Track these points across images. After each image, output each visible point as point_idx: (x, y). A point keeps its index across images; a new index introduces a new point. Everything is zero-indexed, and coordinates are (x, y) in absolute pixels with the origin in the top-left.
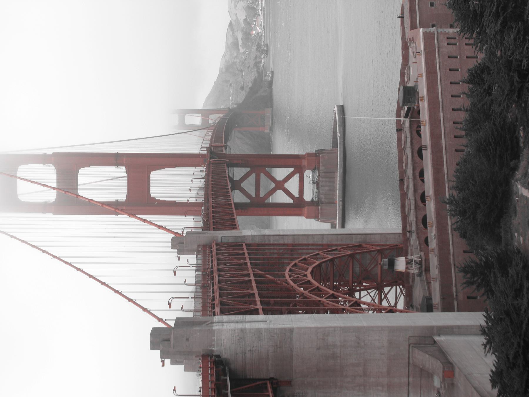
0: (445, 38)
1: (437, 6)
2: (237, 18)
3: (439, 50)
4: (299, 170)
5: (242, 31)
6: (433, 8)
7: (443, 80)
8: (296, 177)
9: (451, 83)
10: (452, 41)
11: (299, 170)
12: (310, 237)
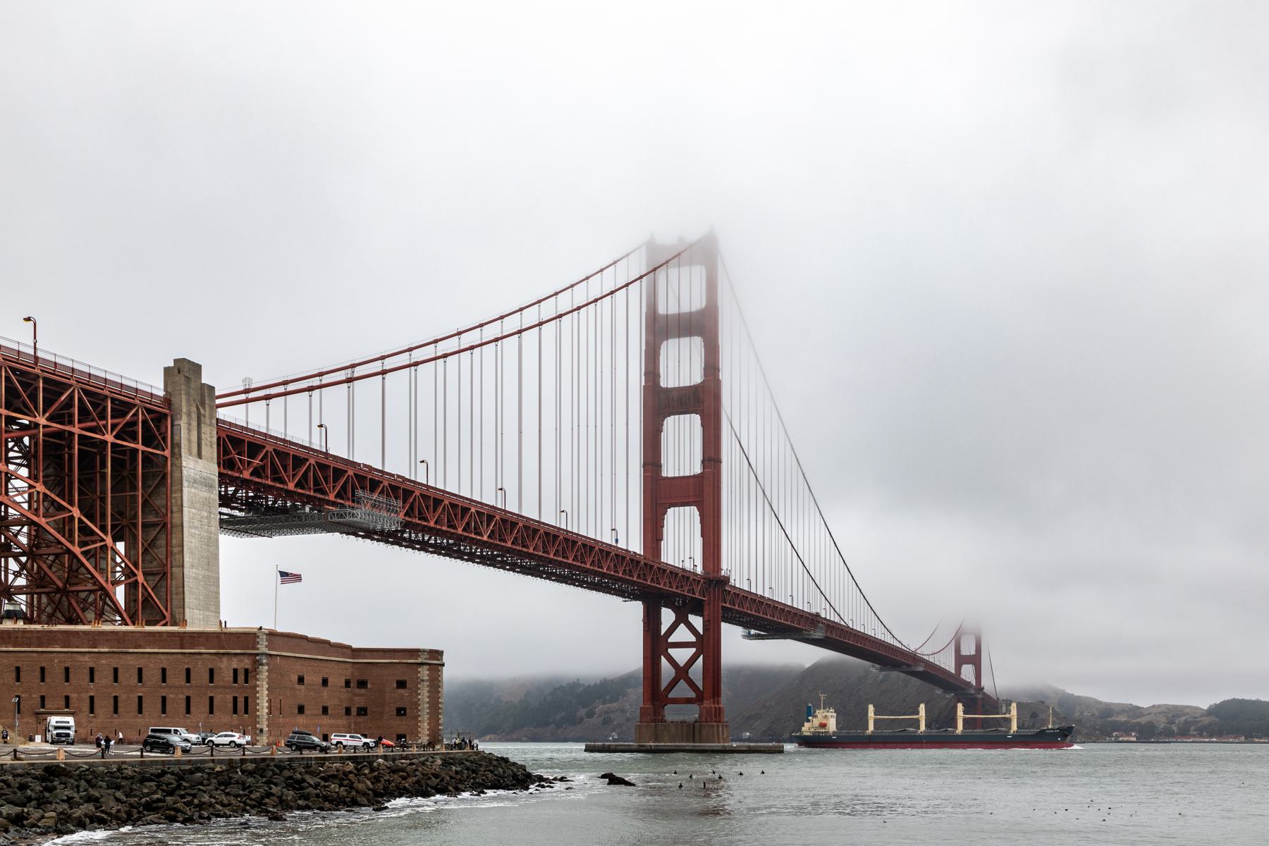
3: (223, 654)
10: (241, 677)
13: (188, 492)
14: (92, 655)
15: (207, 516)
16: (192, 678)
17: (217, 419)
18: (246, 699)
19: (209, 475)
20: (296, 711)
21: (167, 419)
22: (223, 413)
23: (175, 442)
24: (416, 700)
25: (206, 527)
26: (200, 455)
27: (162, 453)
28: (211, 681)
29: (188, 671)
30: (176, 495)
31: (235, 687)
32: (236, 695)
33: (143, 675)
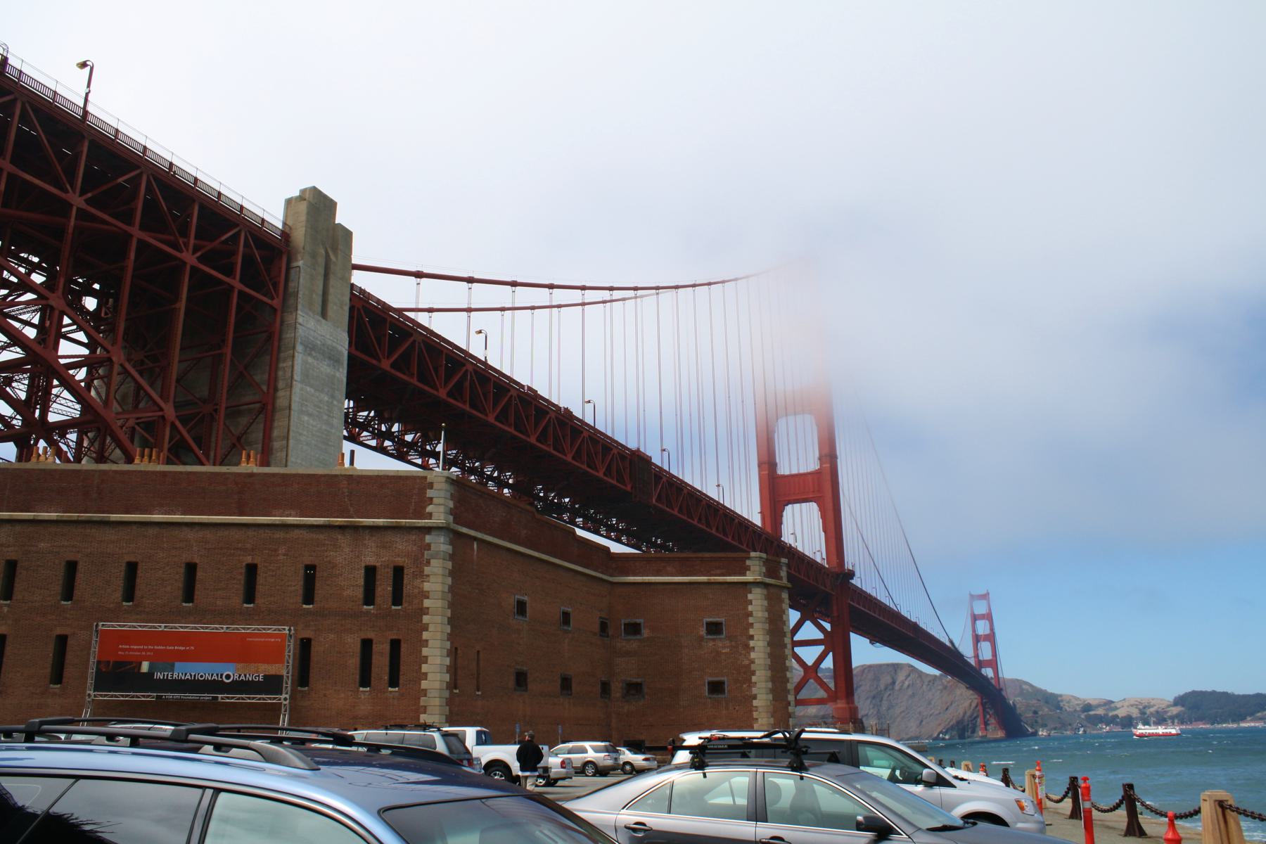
0: (400, 561)
1: (711, 644)
2: (1120, 708)
3: (342, 528)
4: (832, 697)
5: (1105, 715)
6: (703, 631)
7: (208, 534)
8: (822, 694)
9: (191, 569)
10: (384, 588)
11: (832, 697)
12: (285, 442)
13: (300, 359)
14: (18, 528)
15: (327, 402)
16: (261, 588)
17: (352, 285)
18: (395, 645)
19: (334, 344)
20: (511, 683)
21: (281, 258)
22: (358, 278)
23: (291, 290)
24: (746, 662)
25: (325, 417)
26: (324, 314)
27: (269, 301)
28: (309, 597)
29: (252, 570)
30: (285, 365)
31: (368, 612)
32: (370, 635)
33: (138, 580)
